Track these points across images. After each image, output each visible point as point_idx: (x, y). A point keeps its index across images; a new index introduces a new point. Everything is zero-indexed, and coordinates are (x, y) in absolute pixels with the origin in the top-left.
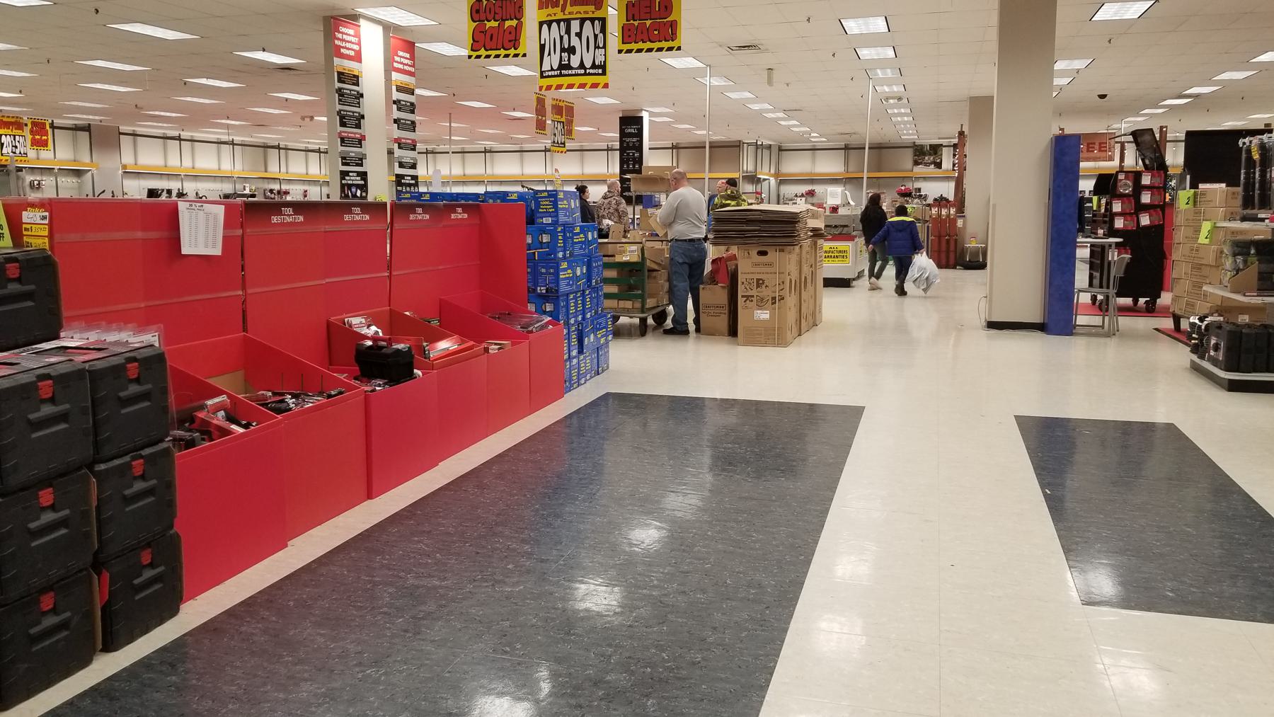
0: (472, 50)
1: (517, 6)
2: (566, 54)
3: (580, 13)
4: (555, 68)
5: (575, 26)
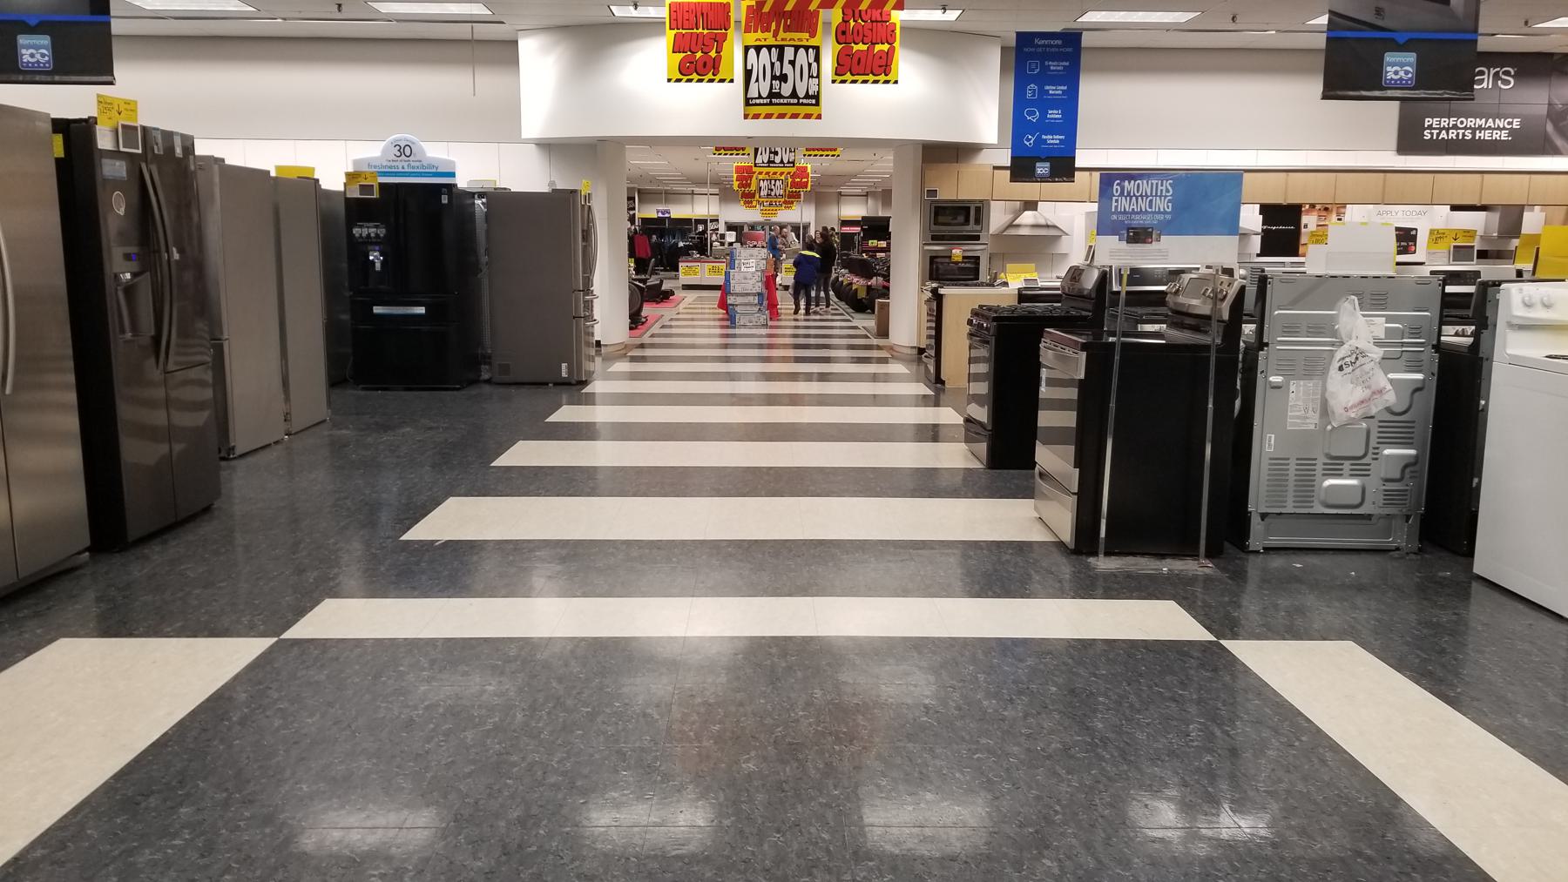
0: (836, 74)
3: (794, 40)
4: (764, 95)
5: (789, 53)
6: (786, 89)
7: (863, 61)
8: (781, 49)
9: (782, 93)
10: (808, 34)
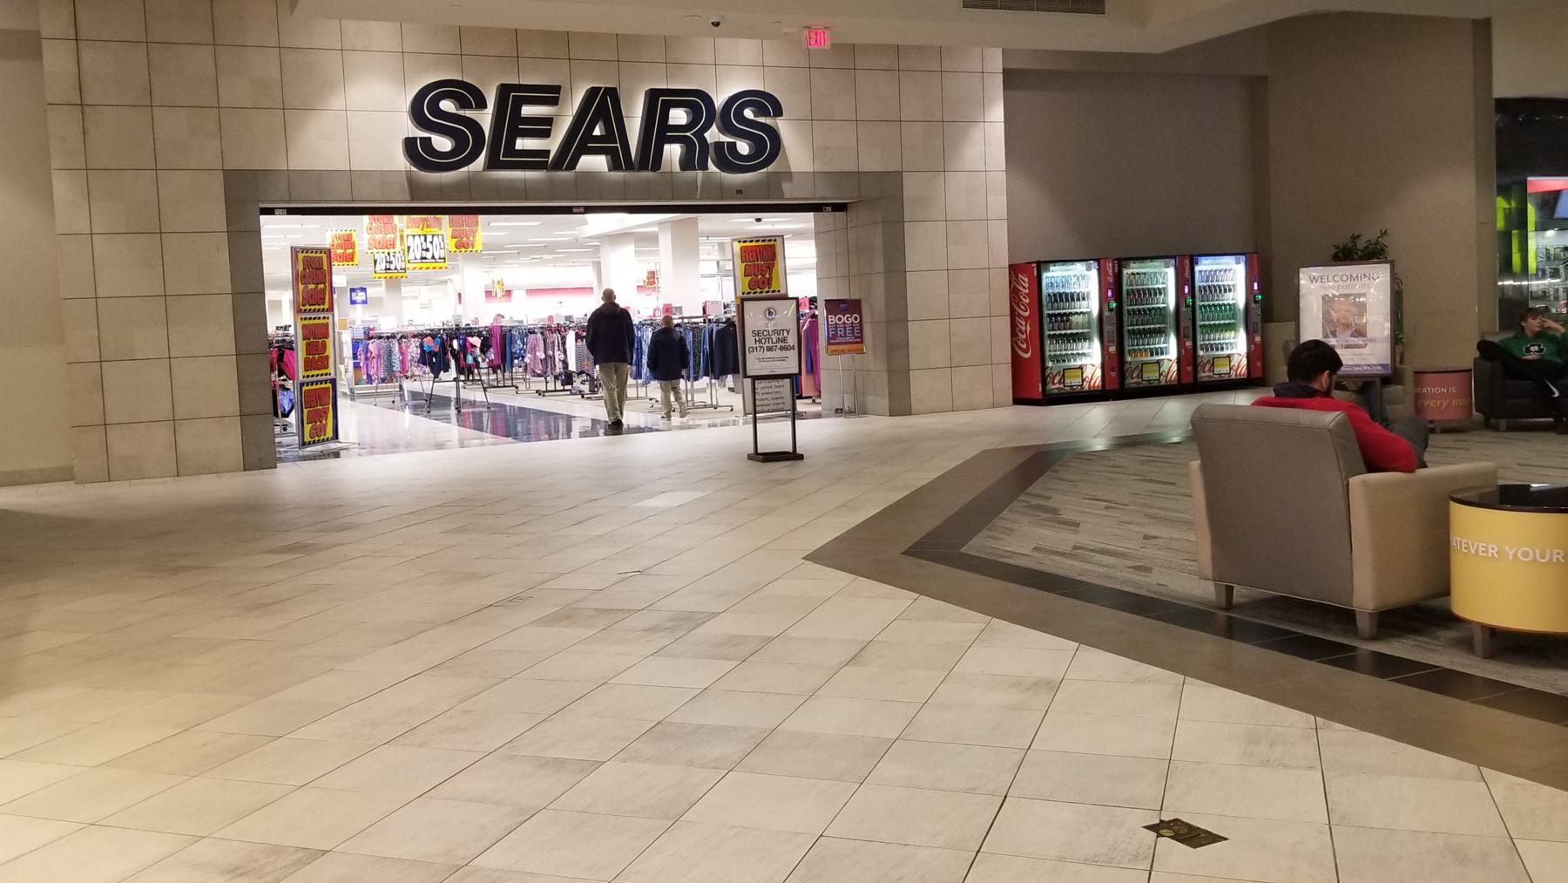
5: (429, 238)
8: (425, 236)
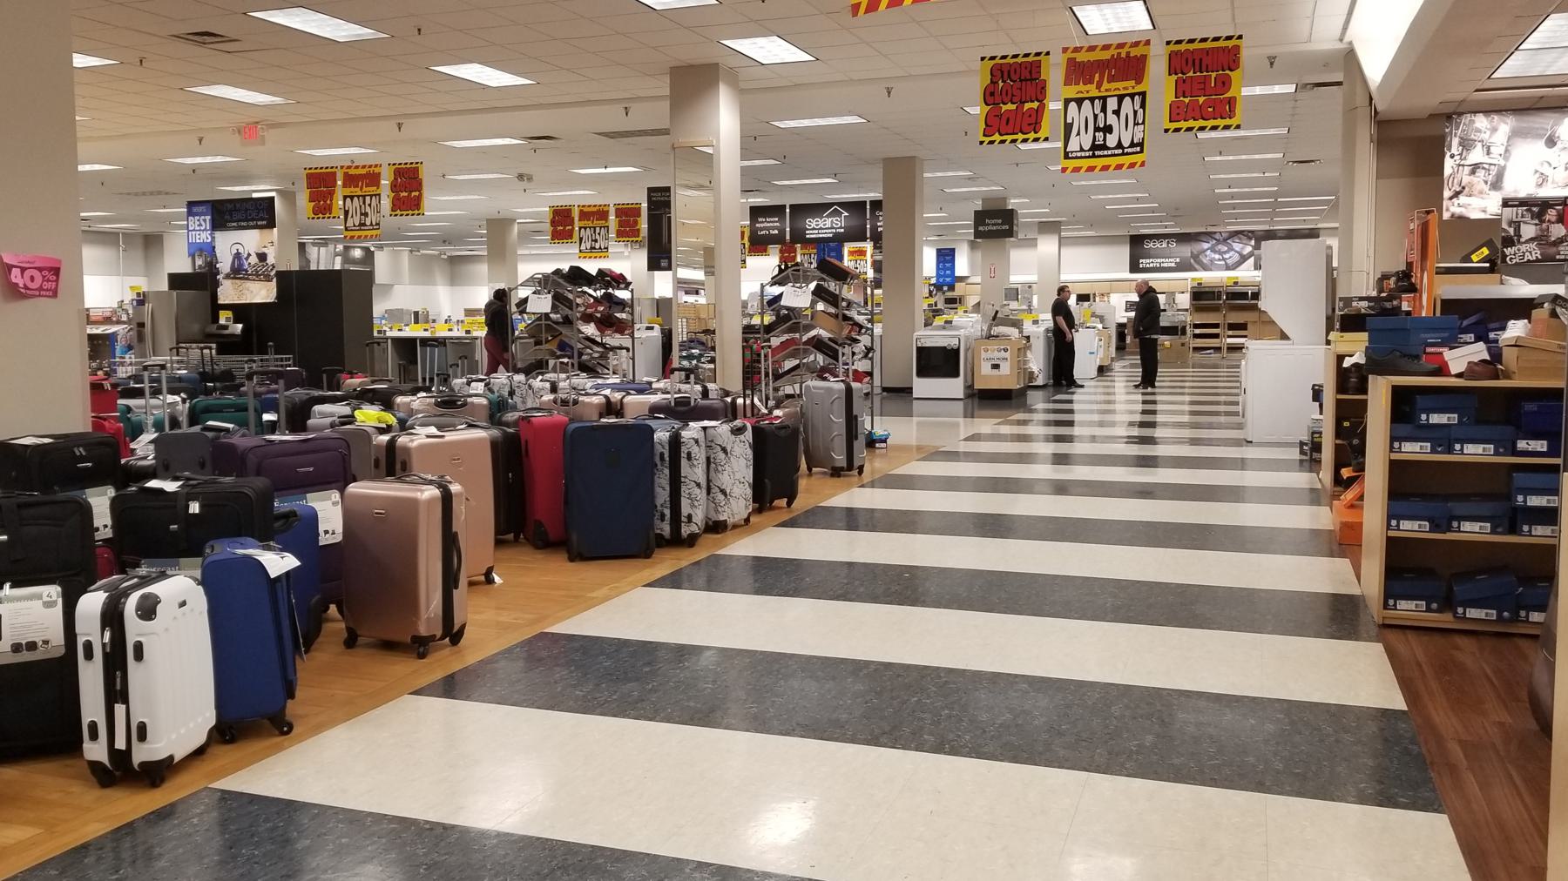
1: (1039, 88)
2: (1101, 134)
3: (1119, 90)
6: (1112, 141)
7: (1011, 121)
9: (1108, 144)
10: (1134, 81)
